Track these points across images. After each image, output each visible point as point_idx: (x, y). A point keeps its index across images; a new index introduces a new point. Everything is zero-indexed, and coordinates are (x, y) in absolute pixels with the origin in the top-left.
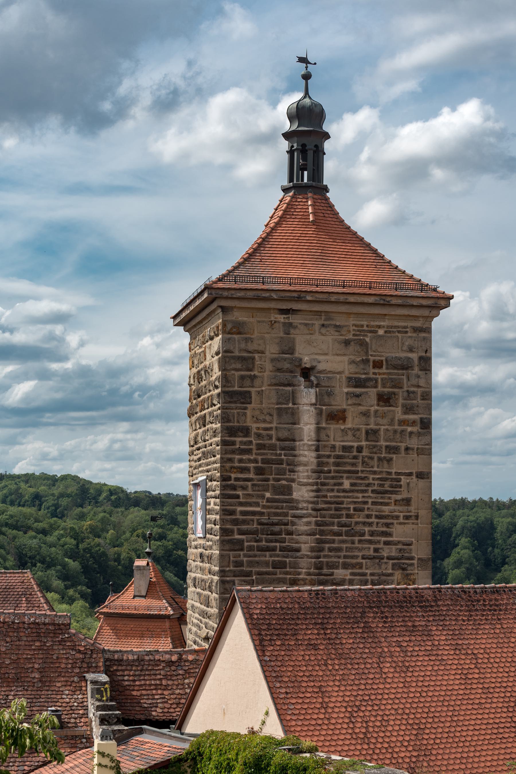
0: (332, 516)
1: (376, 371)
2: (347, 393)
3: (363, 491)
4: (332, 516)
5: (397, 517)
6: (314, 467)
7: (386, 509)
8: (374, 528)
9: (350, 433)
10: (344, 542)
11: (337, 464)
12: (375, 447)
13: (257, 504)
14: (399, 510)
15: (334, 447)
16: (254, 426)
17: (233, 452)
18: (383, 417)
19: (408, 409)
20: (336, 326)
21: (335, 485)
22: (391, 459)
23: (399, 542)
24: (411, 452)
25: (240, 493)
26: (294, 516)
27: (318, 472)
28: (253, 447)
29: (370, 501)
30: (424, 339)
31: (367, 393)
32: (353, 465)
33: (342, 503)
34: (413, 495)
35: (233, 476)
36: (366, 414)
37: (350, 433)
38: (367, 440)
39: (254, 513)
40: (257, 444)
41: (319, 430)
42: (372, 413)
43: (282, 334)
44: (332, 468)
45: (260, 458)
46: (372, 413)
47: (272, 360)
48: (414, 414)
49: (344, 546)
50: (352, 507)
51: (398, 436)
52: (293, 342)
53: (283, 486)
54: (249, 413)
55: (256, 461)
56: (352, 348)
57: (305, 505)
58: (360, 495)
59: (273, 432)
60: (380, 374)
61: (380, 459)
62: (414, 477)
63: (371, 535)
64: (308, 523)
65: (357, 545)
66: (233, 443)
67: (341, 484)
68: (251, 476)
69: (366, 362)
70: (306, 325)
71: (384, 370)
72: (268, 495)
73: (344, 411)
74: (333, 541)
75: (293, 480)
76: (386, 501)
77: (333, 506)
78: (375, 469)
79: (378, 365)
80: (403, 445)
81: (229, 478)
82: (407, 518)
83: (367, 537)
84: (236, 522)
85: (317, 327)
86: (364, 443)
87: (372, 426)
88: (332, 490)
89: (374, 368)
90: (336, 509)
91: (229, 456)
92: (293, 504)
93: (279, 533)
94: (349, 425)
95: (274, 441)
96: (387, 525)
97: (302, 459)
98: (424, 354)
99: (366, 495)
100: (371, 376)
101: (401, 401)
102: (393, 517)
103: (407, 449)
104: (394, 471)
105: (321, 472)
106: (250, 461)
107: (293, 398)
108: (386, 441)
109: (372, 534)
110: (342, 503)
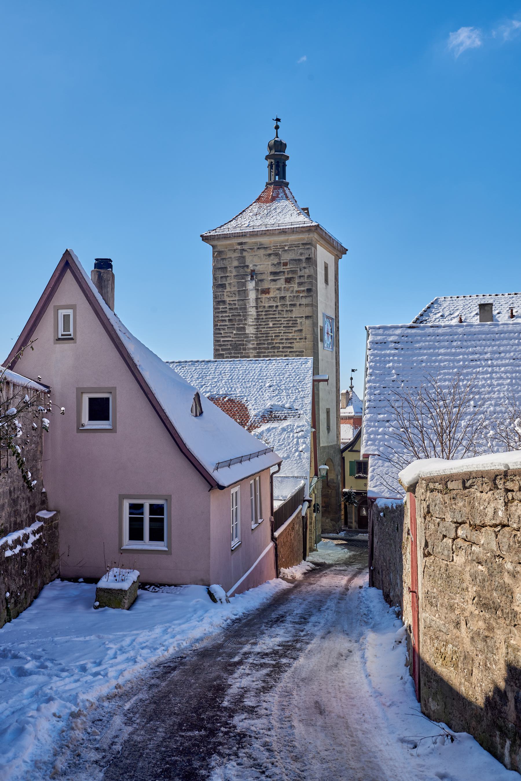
0: (264, 340)
1: (285, 267)
2: (271, 280)
3: (278, 327)
4: (264, 340)
5: (296, 339)
6: (256, 317)
7: (290, 335)
8: (284, 345)
9: (272, 300)
10: (269, 352)
11: (266, 315)
12: (284, 305)
13: (230, 337)
14: (296, 335)
15: (264, 307)
16: (227, 299)
17: (218, 312)
18: (288, 290)
19: (300, 284)
20: (264, 248)
21: (265, 325)
22: (292, 310)
23: (297, 351)
24: (302, 306)
25: (222, 332)
26: (246, 341)
27: (257, 319)
28: (227, 310)
29: (282, 332)
30: (308, 248)
31: (280, 279)
32: (274, 314)
33: (269, 333)
34: (303, 328)
35: (219, 324)
36: (279, 289)
37: (272, 300)
38: (280, 302)
39: (228, 341)
40: (229, 308)
41: (257, 299)
42: (283, 288)
43: (240, 255)
44: (264, 317)
45: (230, 315)
46: (283, 288)
47: (235, 267)
48: (305, 287)
49: (270, 354)
50: (274, 335)
51: (295, 299)
52: (244, 257)
53: (242, 327)
54: (225, 294)
55: (229, 316)
56: (272, 257)
57: (252, 335)
58: (278, 329)
59: (236, 302)
60: (286, 269)
61: (287, 311)
62: (304, 319)
63: (283, 349)
64: (253, 344)
65: (276, 354)
66: (219, 308)
67: (269, 324)
68: (227, 323)
69: (279, 264)
70: (250, 249)
71: (288, 267)
72: (235, 332)
73: (269, 288)
74: (265, 352)
75: (246, 324)
76: (290, 331)
77: (265, 335)
78: (285, 316)
79: (285, 264)
80: (298, 303)
81: (217, 325)
82: (300, 339)
83: (281, 350)
84: (220, 345)
85: (256, 249)
86: (279, 304)
87: (283, 295)
88: (264, 328)
89: (283, 266)
90: (266, 336)
91: (217, 315)
92: (246, 335)
93: (240, 350)
94: (272, 295)
95: (237, 306)
96: (291, 343)
97: (250, 313)
98: (308, 257)
99: (280, 329)
100: (282, 270)
101: (297, 281)
102: (293, 339)
103: (300, 305)
104: (294, 316)
105: (259, 319)
106: (226, 316)
107: (244, 284)
108: (290, 301)
109: (283, 348)
110: (269, 333)
